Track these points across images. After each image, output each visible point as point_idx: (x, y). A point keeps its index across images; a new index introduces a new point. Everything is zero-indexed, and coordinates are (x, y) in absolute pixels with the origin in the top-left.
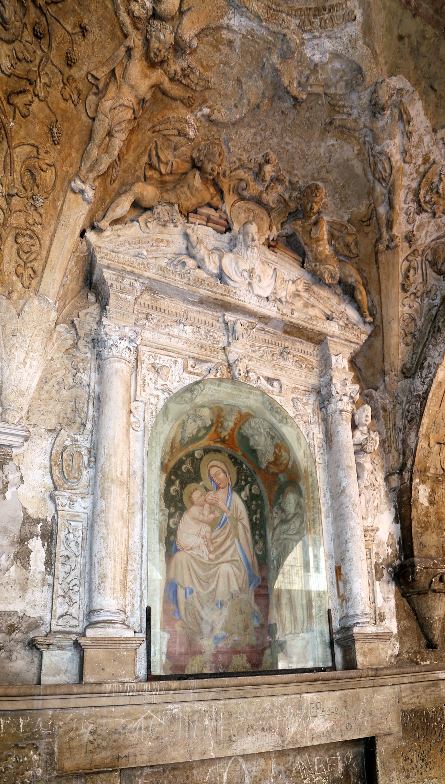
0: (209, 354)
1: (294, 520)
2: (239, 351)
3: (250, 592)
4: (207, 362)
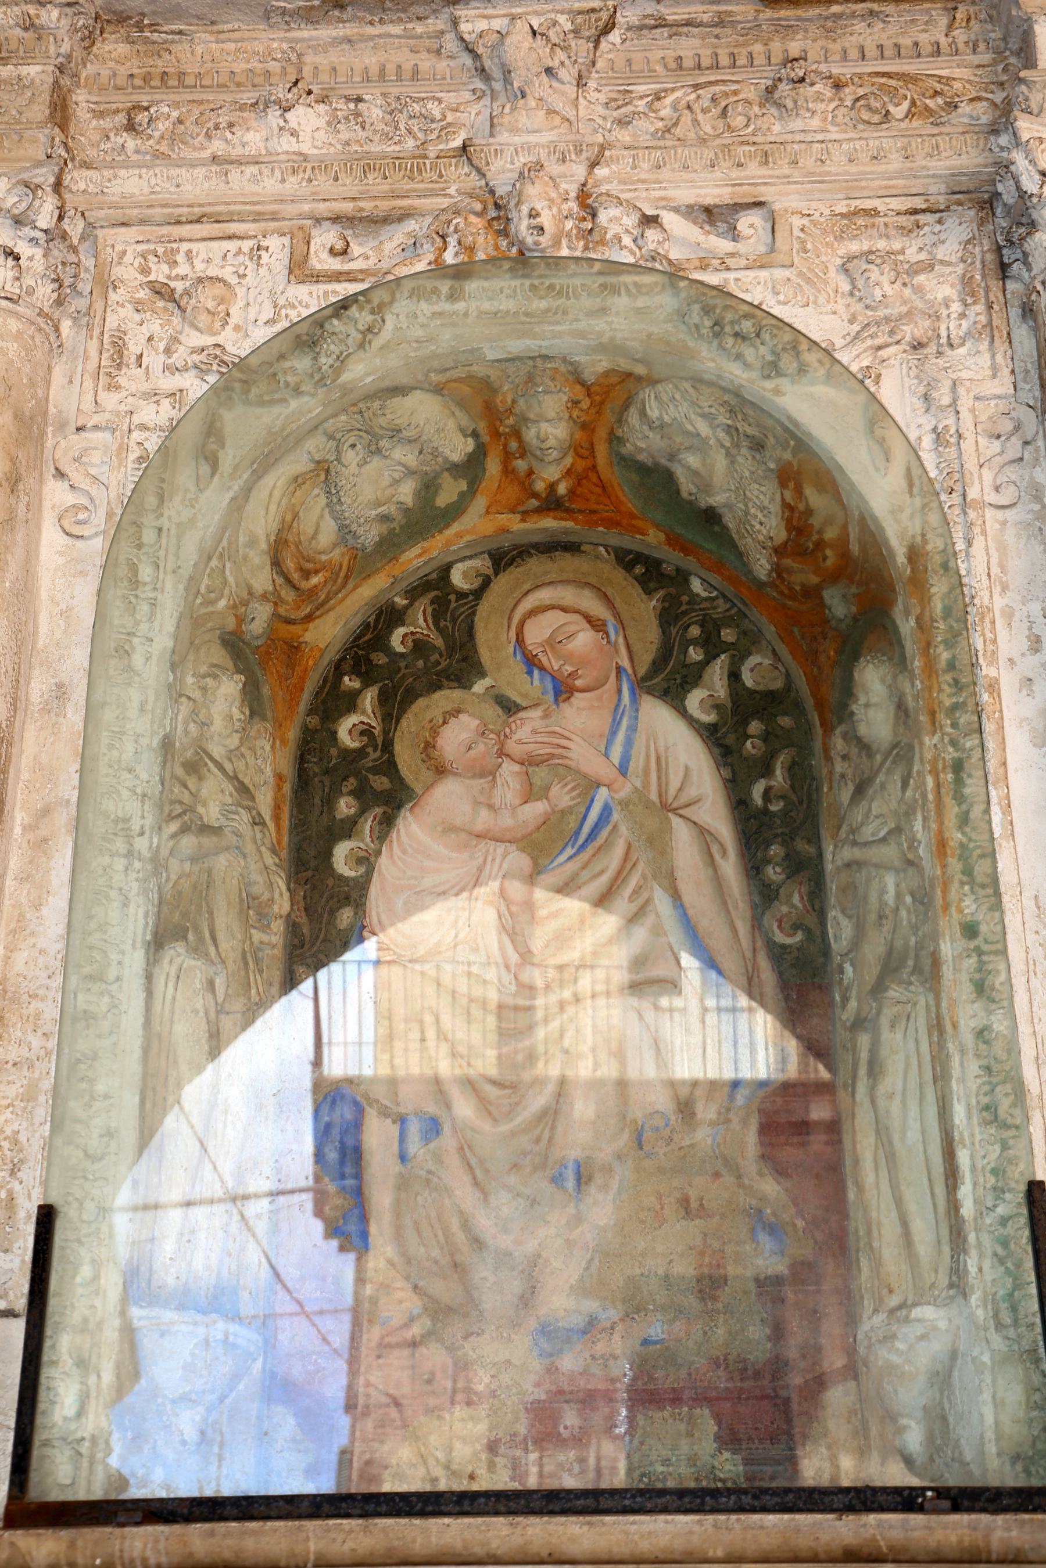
0: (406, 185)
2: (532, 139)
4: (400, 219)
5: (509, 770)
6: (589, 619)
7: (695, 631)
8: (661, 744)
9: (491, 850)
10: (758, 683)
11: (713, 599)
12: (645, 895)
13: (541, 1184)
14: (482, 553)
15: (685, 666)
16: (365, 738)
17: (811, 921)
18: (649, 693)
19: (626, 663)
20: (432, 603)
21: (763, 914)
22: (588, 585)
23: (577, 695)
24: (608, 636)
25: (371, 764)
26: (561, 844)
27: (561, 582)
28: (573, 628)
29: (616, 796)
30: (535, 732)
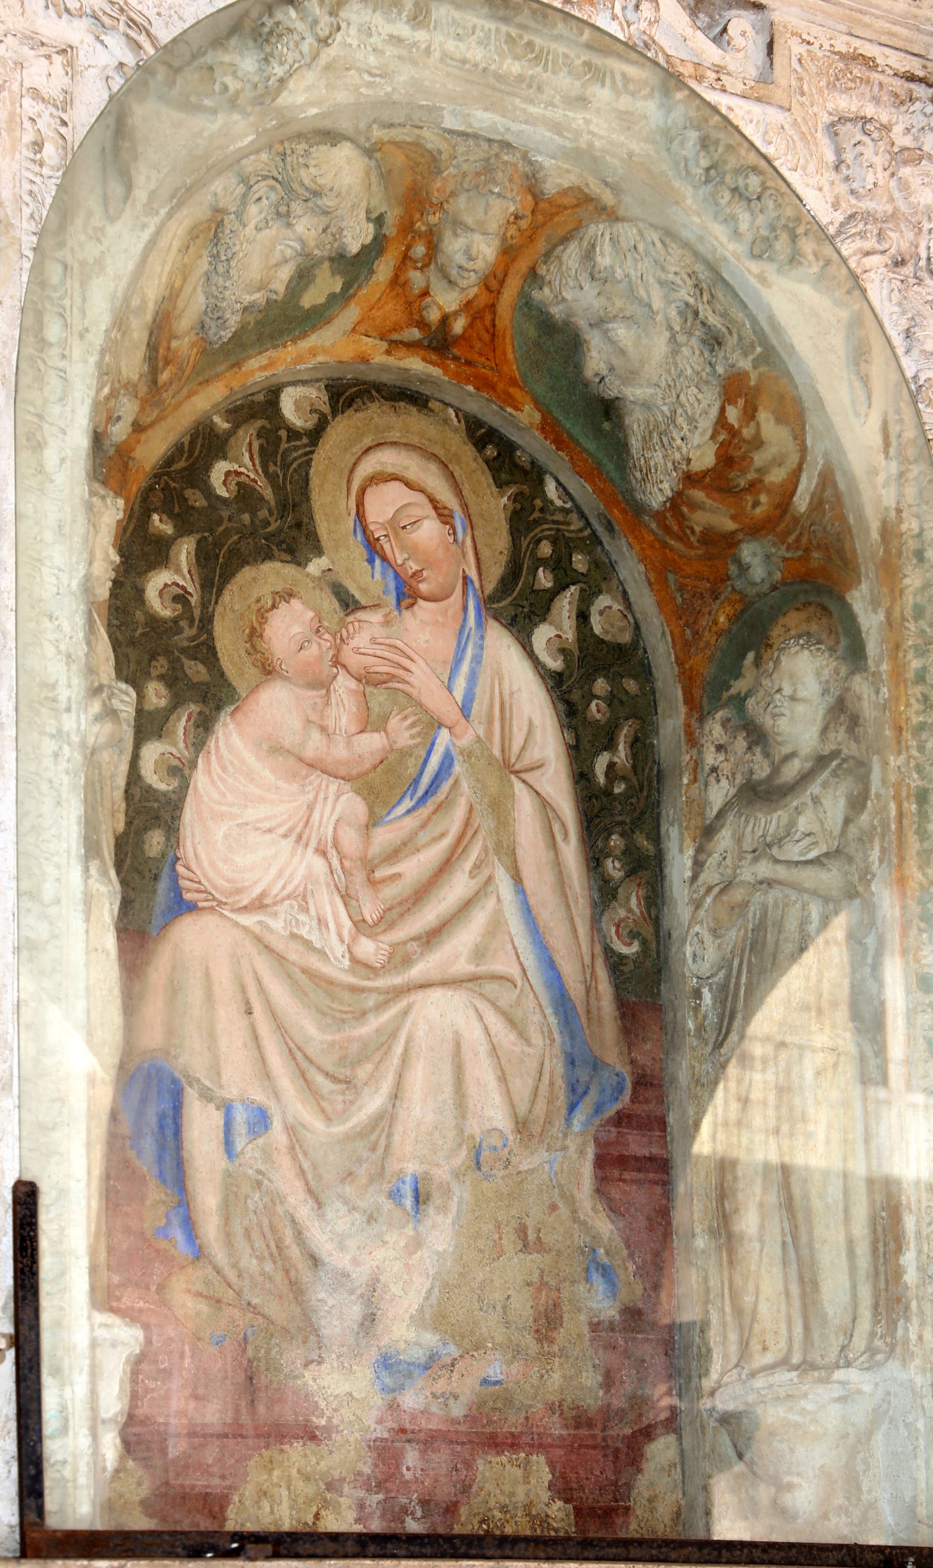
1: (815, 788)
3: (572, 1144)
5: (344, 684)
6: (434, 502)
7: (546, 549)
8: (506, 686)
9: (323, 787)
10: (607, 632)
11: (567, 511)
12: (486, 873)
13: (377, 1198)
14: (317, 380)
15: (533, 591)
16: (180, 606)
17: (648, 931)
18: (496, 618)
19: (473, 574)
20: (259, 436)
21: (602, 914)
22: (434, 457)
23: (421, 602)
24: (455, 533)
25: (185, 644)
26: (398, 792)
27: (405, 445)
28: (417, 512)
29: (458, 743)
30: (373, 641)
